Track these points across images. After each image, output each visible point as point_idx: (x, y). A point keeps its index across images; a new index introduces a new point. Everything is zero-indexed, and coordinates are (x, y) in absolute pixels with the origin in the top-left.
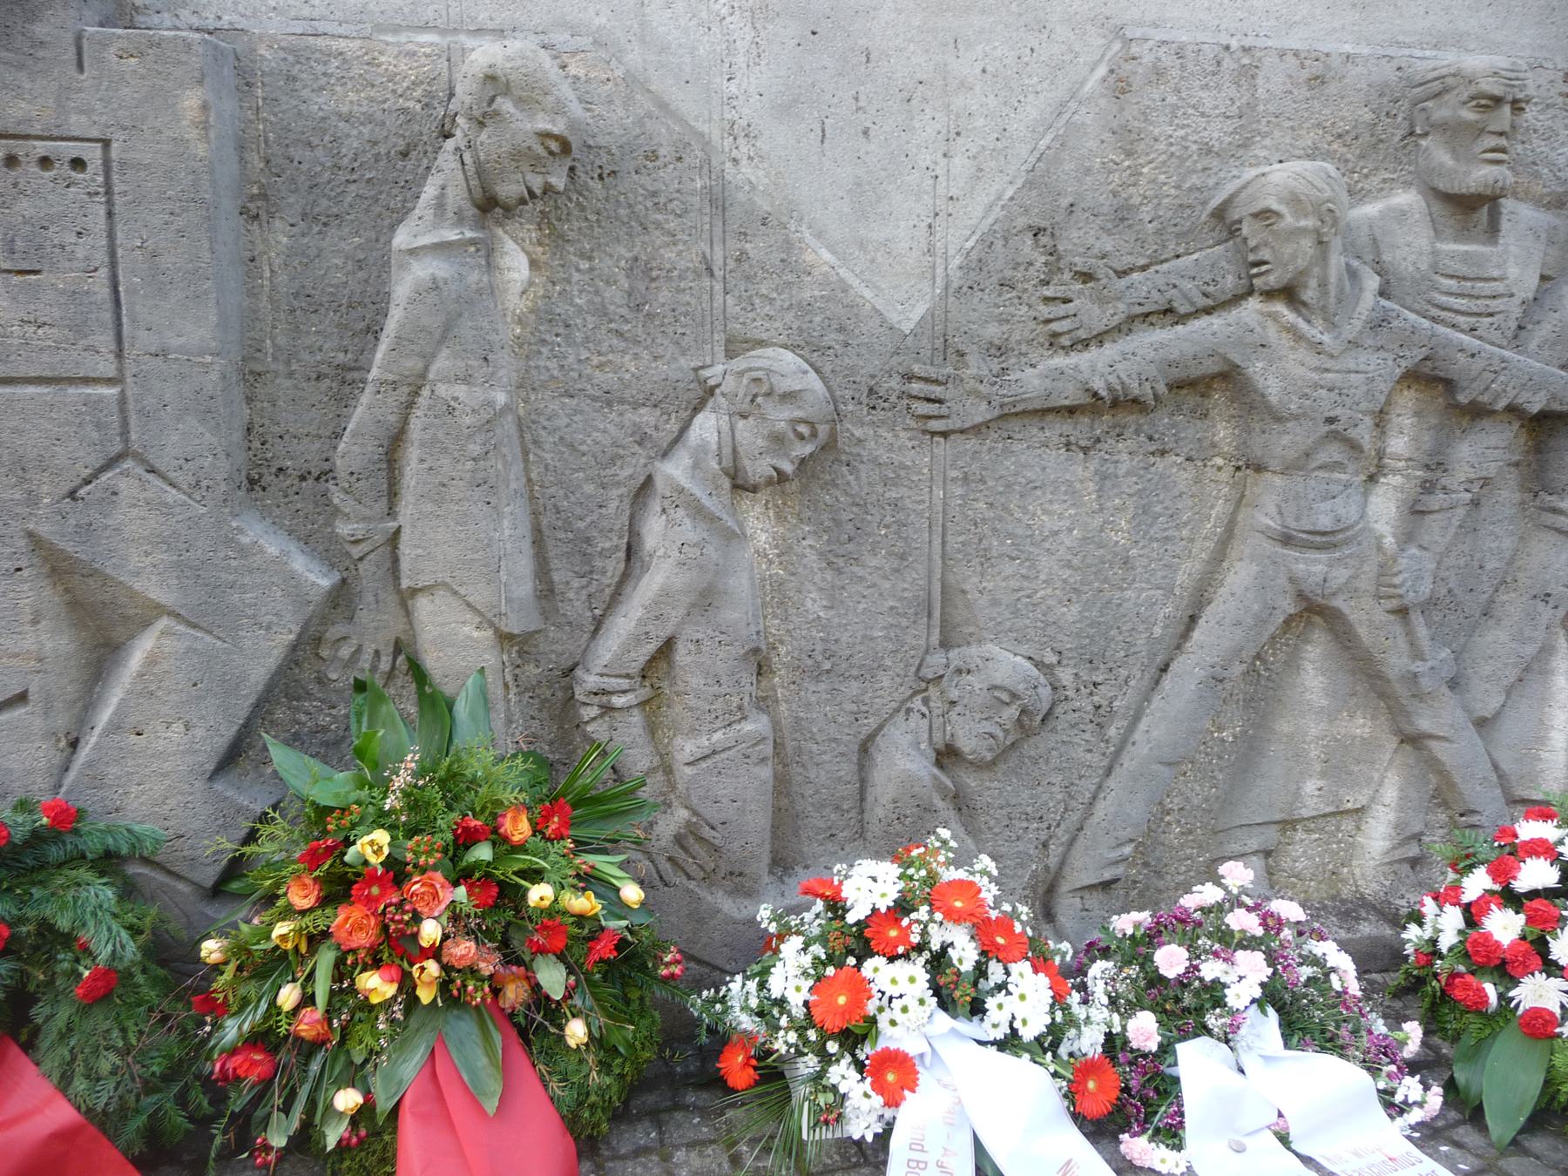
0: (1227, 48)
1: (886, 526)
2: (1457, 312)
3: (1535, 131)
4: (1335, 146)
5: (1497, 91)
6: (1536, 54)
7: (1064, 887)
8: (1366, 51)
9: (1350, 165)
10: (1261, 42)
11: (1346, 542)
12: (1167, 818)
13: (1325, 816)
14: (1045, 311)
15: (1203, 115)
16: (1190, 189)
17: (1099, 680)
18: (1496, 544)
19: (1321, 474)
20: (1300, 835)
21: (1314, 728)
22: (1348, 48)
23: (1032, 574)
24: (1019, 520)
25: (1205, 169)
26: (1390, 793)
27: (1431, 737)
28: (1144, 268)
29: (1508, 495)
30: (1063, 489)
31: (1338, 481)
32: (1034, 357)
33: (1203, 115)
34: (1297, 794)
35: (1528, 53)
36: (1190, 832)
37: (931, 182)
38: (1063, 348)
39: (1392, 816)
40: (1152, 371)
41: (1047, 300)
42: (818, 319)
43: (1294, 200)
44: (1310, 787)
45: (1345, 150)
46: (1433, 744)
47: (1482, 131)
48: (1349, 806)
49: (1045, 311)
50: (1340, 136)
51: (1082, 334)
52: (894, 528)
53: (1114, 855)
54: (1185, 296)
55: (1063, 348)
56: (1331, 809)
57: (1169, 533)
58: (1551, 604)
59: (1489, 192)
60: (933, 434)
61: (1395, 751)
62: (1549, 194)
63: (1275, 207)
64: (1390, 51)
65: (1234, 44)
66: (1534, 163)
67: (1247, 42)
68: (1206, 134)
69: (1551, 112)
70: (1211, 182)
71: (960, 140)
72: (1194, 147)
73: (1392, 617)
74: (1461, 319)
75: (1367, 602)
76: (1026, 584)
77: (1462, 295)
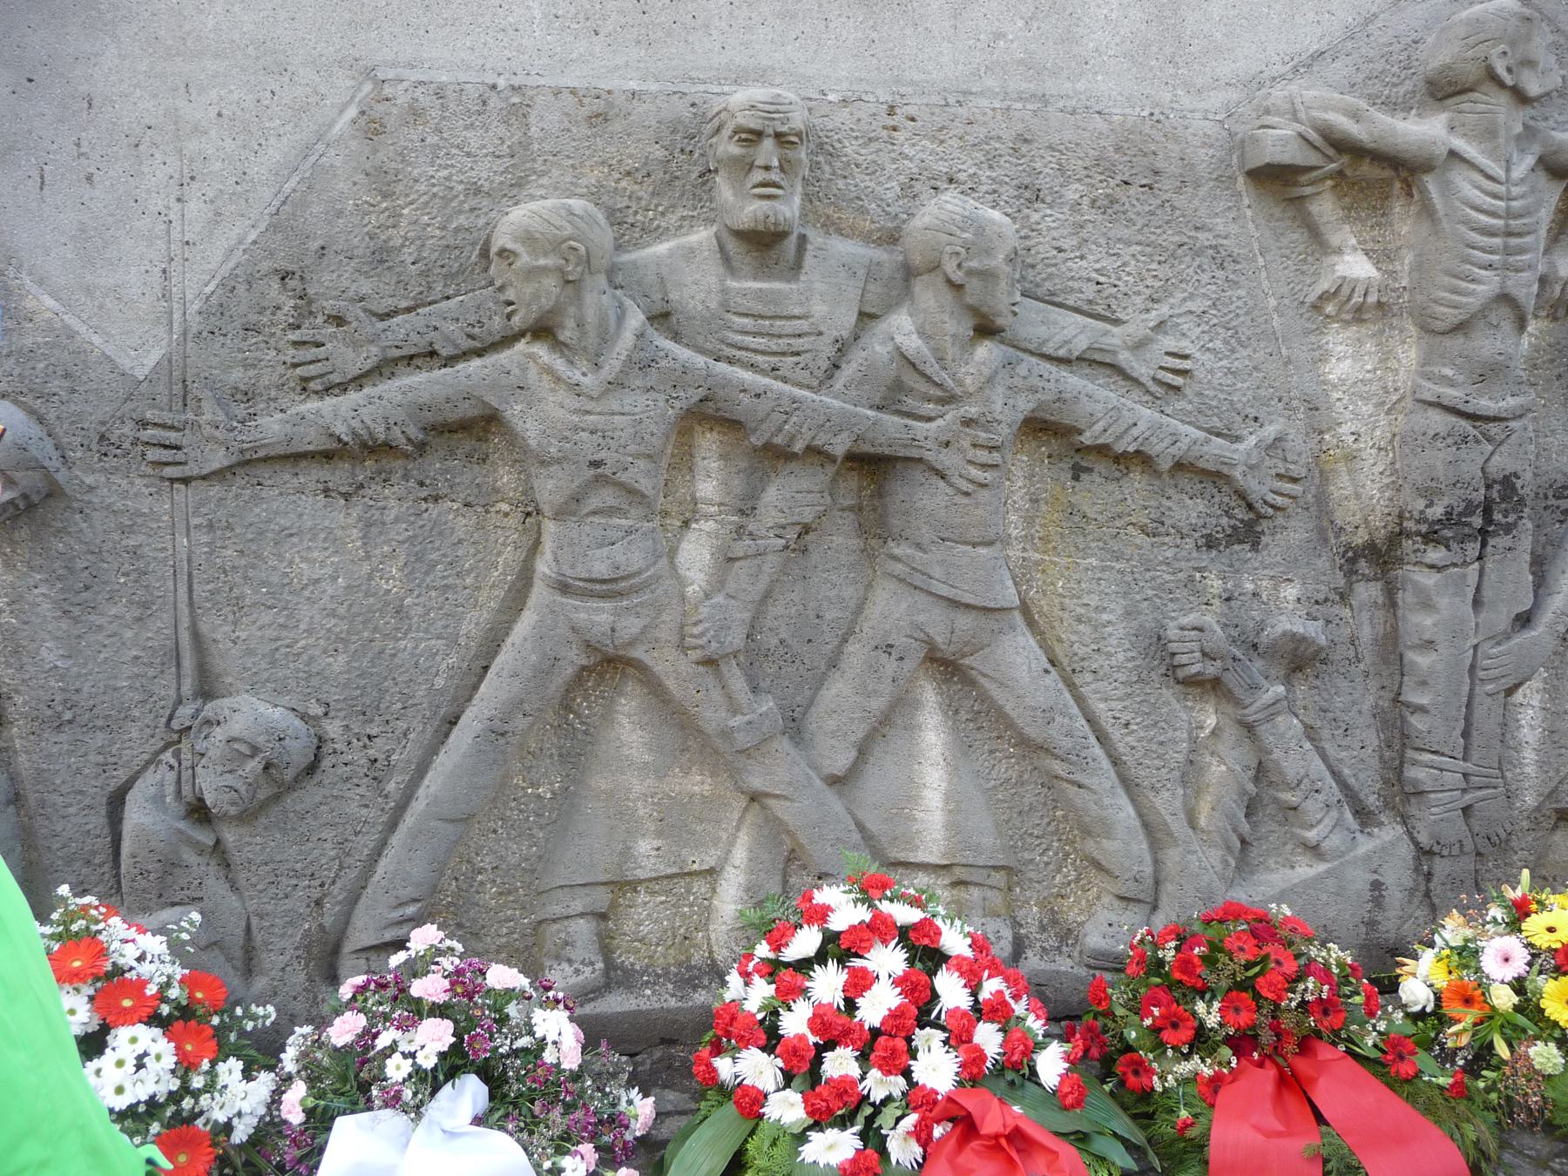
0: (494, 87)
1: (126, 574)
2: (755, 351)
3: (857, 166)
4: (623, 184)
5: (754, 124)
6: (855, 87)
7: (347, 948)
8: (654, 87)
9: (643, 203)
10: (533, 81)
11: (636, 590)
12: (480, 877)
13: (668, 877)
14: (290, 354)
15: (468, 154)
16: (457, 230)
17: (373, 733)
18: (834, 592)
19: (596, 519)
20: (643, 897)
21: (638, 786)
22: (634, 85)
23: (291, 623)
24: (274, 568)
25: (473, 210)
26: (740, 855)
27: (767, 795)
28: (409, 310)
29: (841, 540)
30: (322, 536)
31: (618, 527)
32: (284, 402)
33: (468, 154)
34: (627, 853)
35: (845, 86)
36: (510, 893)
37: (164, 227)
38: (316, 392)
39: (741, 879)
40: (399, 415)
41: (296, 344)
42: (41, 365)
43: (528, 238)
44: (644, 846)
45: (636, 187)
46: (772, 802)
47: (751, 166)
48: (695, 867)
49: (290, 354)
50: (629, 174)
51: (336, 378)
52: (134, 576)
53: (395, 915)
54: (447, 339)
55: (316, 392)
56: (674, 870)
57: (450, 581)
58: (894, 656)
59: (761, 227)
60: (172, 480)
61: (746, 809)
62: (879, 230)
63: (510, 246)
64: (683, 88)
65: (501, 83)
66: (859, 198)
67: (516, 81)
68: (473, 173)
69: (874, 146)
70: (481, 222)
71: (195, 185)
72: (460, 187)
73: (701, 669)
74: (760, 358)
75: (671, 654)
76: (285, 633)
77: (762, 335)
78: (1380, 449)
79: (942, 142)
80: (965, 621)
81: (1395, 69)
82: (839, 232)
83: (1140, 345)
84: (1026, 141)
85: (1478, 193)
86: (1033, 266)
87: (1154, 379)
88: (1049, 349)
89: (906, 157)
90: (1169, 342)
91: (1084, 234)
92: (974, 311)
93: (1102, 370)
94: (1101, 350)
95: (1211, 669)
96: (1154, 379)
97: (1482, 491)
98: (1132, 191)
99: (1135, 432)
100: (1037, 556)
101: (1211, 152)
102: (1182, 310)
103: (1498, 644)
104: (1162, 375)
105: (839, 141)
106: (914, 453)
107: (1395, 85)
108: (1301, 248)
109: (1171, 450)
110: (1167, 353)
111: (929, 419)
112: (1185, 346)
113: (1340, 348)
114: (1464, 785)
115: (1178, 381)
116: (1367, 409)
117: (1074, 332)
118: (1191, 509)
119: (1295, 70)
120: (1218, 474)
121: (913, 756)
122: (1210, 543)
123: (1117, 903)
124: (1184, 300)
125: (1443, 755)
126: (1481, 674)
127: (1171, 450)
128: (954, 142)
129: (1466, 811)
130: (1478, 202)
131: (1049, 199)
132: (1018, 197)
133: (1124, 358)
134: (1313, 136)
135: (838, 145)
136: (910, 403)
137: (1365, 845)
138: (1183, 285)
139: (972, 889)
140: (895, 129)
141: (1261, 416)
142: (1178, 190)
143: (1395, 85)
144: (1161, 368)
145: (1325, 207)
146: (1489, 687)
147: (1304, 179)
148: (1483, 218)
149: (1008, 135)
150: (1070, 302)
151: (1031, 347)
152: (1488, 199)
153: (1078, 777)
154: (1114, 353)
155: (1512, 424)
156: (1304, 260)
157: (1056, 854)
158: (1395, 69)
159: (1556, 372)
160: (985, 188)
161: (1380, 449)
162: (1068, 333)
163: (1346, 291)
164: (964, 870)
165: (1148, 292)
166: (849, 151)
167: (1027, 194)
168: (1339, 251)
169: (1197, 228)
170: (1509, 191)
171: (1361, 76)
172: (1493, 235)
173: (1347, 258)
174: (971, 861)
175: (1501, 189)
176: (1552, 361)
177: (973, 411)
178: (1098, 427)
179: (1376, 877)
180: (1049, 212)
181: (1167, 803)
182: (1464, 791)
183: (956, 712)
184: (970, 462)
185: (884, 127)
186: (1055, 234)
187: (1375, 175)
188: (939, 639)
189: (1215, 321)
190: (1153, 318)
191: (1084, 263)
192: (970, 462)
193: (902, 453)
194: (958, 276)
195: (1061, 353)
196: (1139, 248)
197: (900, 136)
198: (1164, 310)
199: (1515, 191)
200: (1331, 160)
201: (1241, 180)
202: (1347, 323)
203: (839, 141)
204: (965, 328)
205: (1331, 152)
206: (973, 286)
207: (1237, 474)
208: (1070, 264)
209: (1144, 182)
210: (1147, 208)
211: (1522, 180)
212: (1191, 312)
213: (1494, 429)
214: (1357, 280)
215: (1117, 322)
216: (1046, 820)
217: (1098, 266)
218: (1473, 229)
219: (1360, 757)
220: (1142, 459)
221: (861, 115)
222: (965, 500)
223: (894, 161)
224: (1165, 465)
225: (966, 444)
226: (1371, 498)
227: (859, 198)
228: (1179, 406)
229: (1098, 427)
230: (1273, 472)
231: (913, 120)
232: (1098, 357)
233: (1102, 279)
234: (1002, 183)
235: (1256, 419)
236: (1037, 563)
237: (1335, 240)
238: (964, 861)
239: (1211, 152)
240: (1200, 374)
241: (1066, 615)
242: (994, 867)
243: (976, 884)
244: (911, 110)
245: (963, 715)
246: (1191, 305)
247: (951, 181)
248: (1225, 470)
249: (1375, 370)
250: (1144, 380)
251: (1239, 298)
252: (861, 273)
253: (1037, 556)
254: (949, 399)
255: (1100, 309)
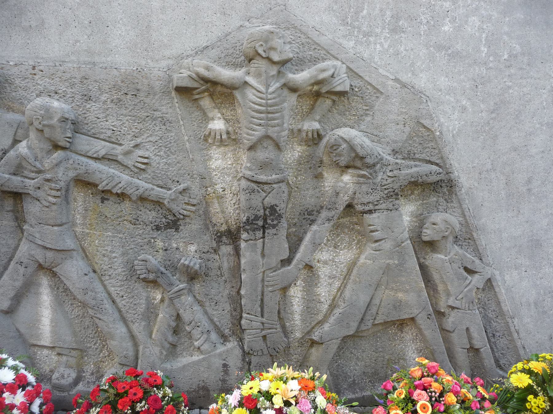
6: (20, 60)
18: (4, 242)
35: (17, 59)
58: (23, 266)
69: (27, 80)
78: (234, 194)
79: (53, 79)
80: (50, 254)
81: (238, 52)
82: (13, 111)
83: (127, 153)
84: (86, 78)
85: (254, 97)
86: (87, 124)
87: (134, 166)
88: (89, 154)
89: (39, 84)
90: (140, 152)
91: (108, 112)
92: (49, 140)
93: (113, 162)
94: (111, 155)
95: (151, 277)
96: (134, 166)
97: (262, 211)
98: (129, 97)
99: (120, 185)
100: (88, 231)
101: (161, 82)
102: (148, 140)
103: (274, 271)
104: (137, 164)
105: (13, 79)
106: (26, 191)
107: (237, 58)
108: (200, 118)
109: (137, 192)
110: (139, 156)
111: (33, 179)
112: (147, 154)
113: (216, 156)
114: (262, 327)
115: (143, 167)
116: (228, 179)
117: (100, 147)
118: (150, 215)
119: (197, 53)
120: (158, 202)
121: (38, 304)
122: (158, 228)
123: (118, 366)
124: (148, 137)
125: (252, 315)
126: (266, 283)
127: (137, 192)
128: (58, 79)
129: (264, 337)
130: (254, 100)
131: (94, 100)
132: (82, 99)
133: (120, 158)
134: (194, 76)
135: (13, 80)
136: (26, 173)
137: (221, 349)
138: (148, 131)
139: (63, 356)
140: (35, 74)
141: (180, 181)
142: (147, 97)
143: (237, 58)
144: (137, 162)
145: (206, 103)
146: (270, 289)
147: (195, 92)
148: (257, 107)
149: (78, 76)
150: (101, 137)
151: (82, 153)
152: (260, 100)
153: (98, 315)
154: (117, 156)
155: (274, 186)
156: (202, 122)
157: (100, 345)
158: (238, 52)
159: (309, 166)
160: (69, 96)
161: (234, 194)
162: (97, 148)
163: (212, 134)
164: (59, 349)
165: (133, 134)
166: (17, 82)
167: (85, 98)
168: (213, 119)
169: (154, 110)
170: (267, 96)
171: (223, 55)
172: (261, 113)
173: (215, 122)
174: (61, 346)
175: (264, 96)
176: (308, 162)
177: (48, 176)
178: (104, 183)
179: (224, 362)
180: (94, 104)
181: (138, 328)
182: (262, 330)
183: (58, 288)
184: (49, 195)
185: (31, 74)
186: (96, 112)
187: (220, 92)
188: (41, 261)
189: (161, 145)
190: (133, 143)
191: (108, 123)
192: (49, 195)
193: (21, 191)
194: (40, 127)
195: (95, 156)
196: (130, 118)
197: (36, 77)
198: (139, 140)
199: (269, 96)
200: (202, 85)
201: (173, 93)
202: (219, 146)
203: (13, 79)
204: (47, 146)
205: (202, 82)
206: (46, 130)
207: (166, 202)
208: (102, 123)
209: (133, 93)
210: (133, 103)
211: (273, 92)
212: (151, 141)
213: (266, 187)
214: (215, 130)
215: (121, 145)
216: (94, 332)
217: (113, 124)
218: (253, 111)
219: (222, 314)
220: (122, 196)
221: (22, 69)
222: (47, 209)
223: (34, 86)
224: (134, 198)
225: (47, 188)
226: (230, 213)
227: (21, 99)
228: (144, 176)
229: (104, 183)
230: (183, 202)
231: (42, 71)
232: (110, 157)
233: (115, 129)
234: (76, 94)
235: (178, 182)
236: (88, 234)
237: (210, 115)
238: (59, 346)
239: (161, 82)
240: (154, 164)
241: (98, 253)
242: (73, 349)
243: (65, 355)
244: (41, 68)
245: (61, 290)
246: (151, 139)
247: (56, 93)
248: (161, 201)
249: (232, 164)
250: (129, 166)
251: (171, 136)
252: (15, 126)
253: (88, 231)
254: (39, 172)
255: (113, 140)
